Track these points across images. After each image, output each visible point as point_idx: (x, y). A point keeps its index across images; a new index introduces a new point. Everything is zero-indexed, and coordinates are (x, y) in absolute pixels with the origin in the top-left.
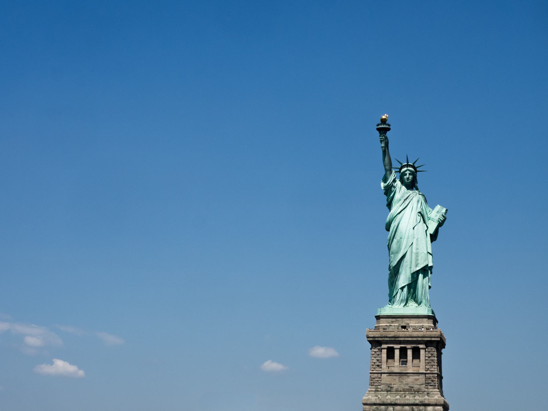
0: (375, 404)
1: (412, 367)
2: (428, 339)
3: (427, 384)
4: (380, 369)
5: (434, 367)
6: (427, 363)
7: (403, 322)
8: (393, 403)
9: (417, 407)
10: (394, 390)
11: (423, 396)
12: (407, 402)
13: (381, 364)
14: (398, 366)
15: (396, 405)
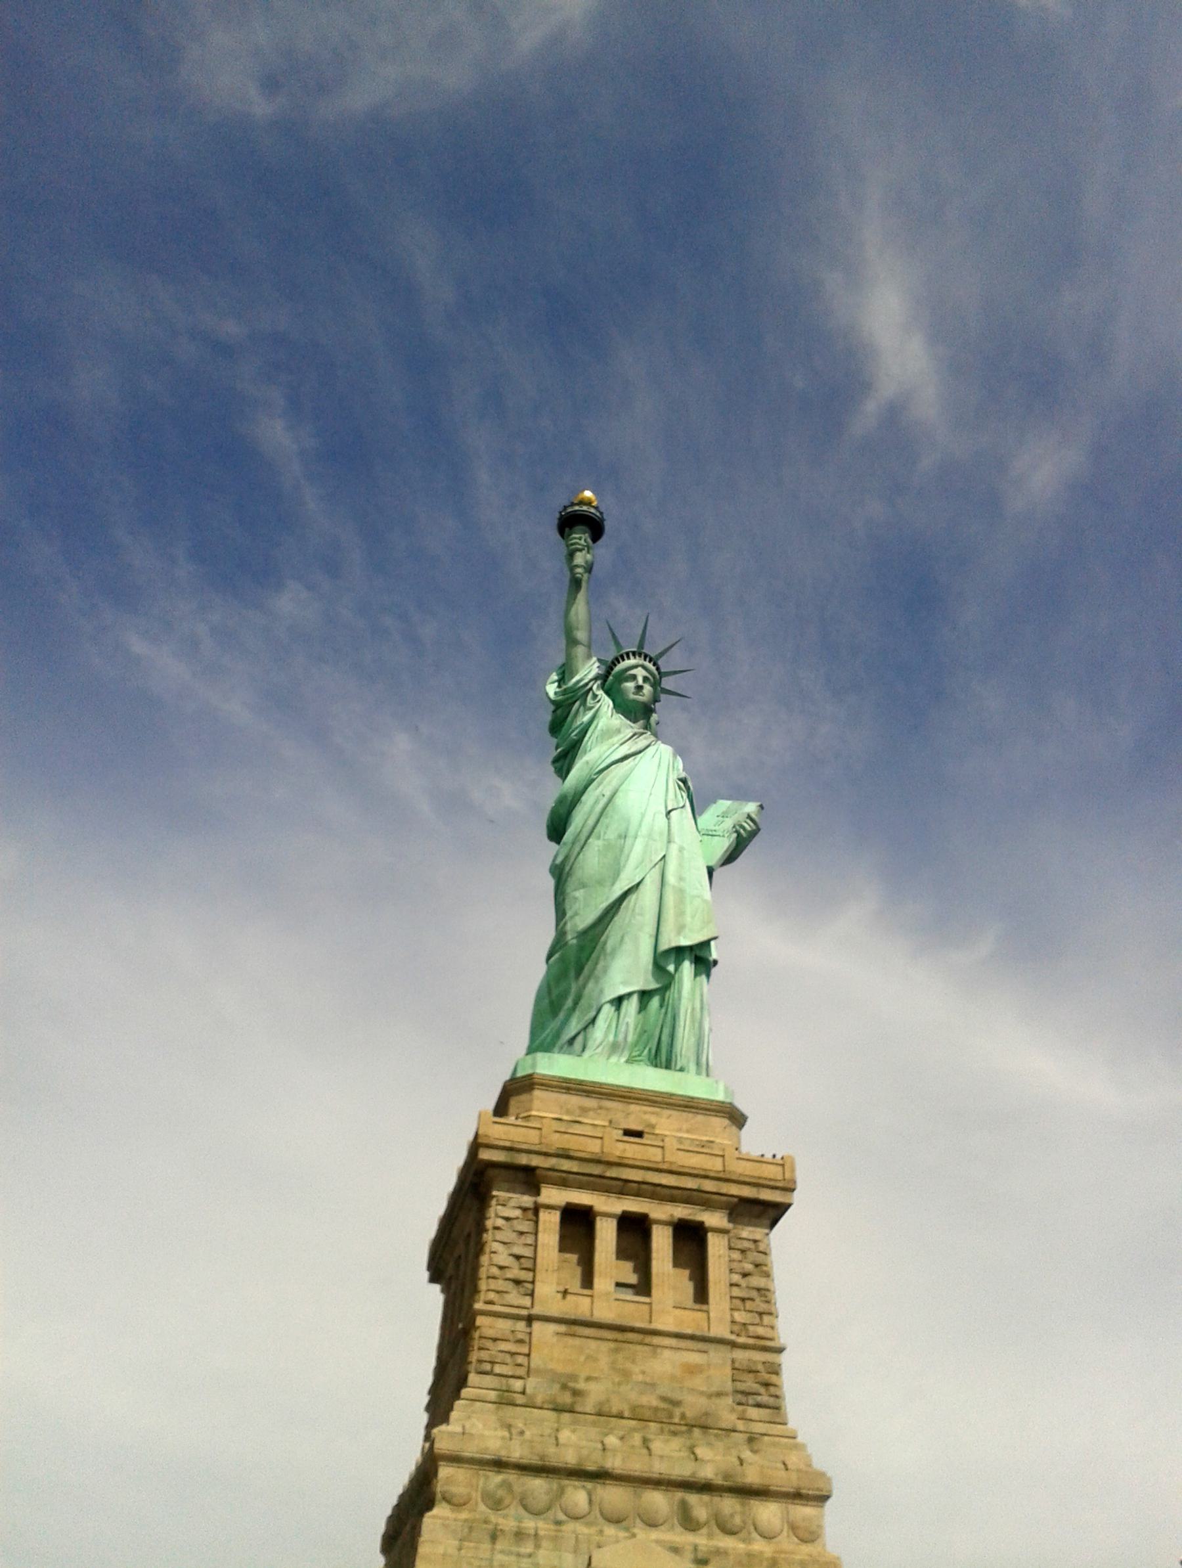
0: (499, 1464)
1: (674, 1307)
2: (747, 1192)
3: (739, 1397)
4: (527, 1301)
5: (766, 1319)
6: (738, 1302)
7: (632, 1117)
8: (591, 1467)
9: (706, 1498)
10: (589, 1405)
11: (729, 1448)
12: (659, 1468)
13: (531, 1274)
14: (608, 1294)
15: (601, 1476)
